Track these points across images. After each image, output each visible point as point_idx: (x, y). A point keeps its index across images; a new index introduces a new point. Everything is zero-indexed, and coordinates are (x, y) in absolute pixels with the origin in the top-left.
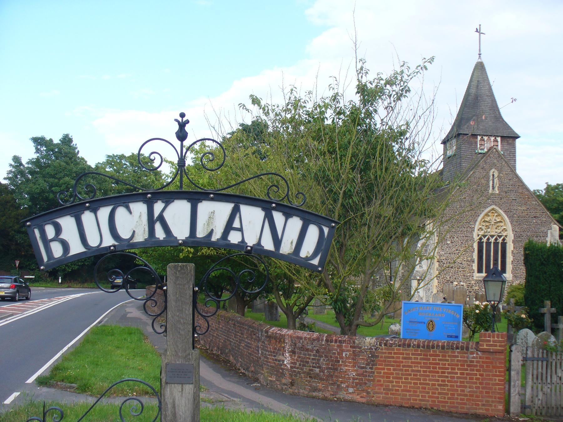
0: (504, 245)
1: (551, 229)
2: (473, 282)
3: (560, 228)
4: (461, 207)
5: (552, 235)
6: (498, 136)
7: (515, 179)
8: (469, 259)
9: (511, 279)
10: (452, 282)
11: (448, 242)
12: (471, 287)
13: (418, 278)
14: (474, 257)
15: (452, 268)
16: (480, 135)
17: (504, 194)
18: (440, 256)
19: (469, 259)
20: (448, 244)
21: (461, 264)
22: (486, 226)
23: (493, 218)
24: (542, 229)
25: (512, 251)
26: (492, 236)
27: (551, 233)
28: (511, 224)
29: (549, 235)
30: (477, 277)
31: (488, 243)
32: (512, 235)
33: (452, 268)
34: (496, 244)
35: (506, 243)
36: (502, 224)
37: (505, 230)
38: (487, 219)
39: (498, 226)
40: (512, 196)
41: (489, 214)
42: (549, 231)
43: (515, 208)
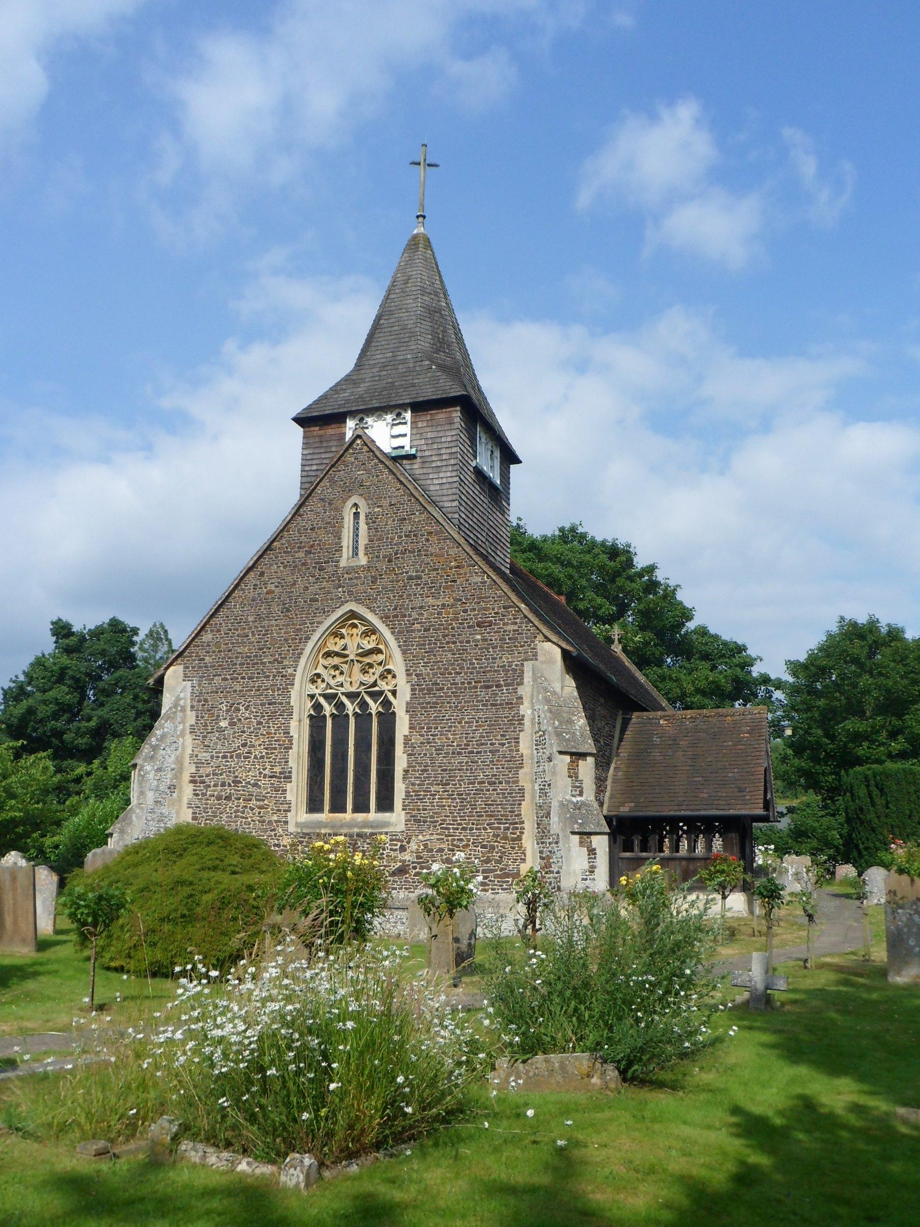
0: (388, 719)
1: (535, 657)
3: (564, 651)
4: (259, 618)
6: (404, 407)
8: (277, 769)
9: (401, 827)
11: (223, 724)
14: (292, 763)
15: (228, 798)
16: (352, 414)
18: (199, 764)
20: (221, 730)
22: (336, 667)
23: (354, 642)
25: (407, 739)
28: (404, 652)
31: (340, 719)
32: (408, 688)
33: (228, 798)
34: (363, 718)
35: (394, 714)
38: (335, 645)
39: (371, 666)
41: (343, 631)
42: (528, 666)
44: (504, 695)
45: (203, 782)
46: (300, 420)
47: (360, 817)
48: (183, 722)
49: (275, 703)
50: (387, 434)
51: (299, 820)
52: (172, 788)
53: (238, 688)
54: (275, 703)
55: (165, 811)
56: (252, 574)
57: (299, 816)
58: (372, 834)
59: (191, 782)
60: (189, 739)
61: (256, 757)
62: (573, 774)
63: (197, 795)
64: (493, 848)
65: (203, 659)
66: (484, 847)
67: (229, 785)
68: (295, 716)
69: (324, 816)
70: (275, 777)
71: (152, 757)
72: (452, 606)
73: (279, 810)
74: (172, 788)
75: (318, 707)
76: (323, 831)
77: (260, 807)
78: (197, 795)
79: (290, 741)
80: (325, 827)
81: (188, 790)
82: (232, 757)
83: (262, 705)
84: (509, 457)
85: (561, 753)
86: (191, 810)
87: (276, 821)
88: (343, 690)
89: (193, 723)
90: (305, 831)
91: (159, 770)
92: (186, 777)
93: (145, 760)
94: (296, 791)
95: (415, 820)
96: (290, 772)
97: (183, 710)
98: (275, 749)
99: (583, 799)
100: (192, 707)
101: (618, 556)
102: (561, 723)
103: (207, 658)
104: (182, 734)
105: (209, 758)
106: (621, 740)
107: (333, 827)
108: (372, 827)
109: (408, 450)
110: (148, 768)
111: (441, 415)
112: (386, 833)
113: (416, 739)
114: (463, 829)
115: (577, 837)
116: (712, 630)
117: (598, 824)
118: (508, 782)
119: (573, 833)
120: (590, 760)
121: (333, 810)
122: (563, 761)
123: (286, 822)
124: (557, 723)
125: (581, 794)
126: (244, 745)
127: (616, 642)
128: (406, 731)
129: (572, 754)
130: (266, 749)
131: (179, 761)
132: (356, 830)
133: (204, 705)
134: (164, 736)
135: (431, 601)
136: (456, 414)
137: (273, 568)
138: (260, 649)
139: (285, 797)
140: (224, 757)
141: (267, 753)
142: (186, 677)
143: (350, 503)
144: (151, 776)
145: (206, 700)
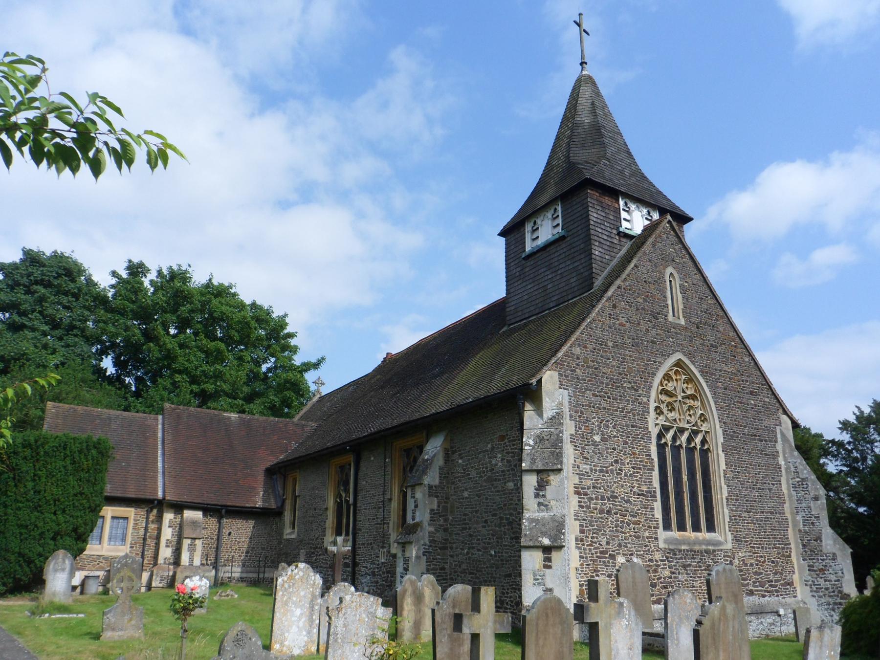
2: (658, 556)
7: (711, 301)
9: (729, 546)
10: (613, 557)
11: (597, 438)
12: (655, 571)
13: (546, 541)
17: (694, 329)
18: (581, 475)
19: (644, 488)
20: (595, 444)
21: (628, 501)
24: (766, 423)
26: (682, 430)
29: (779, 436)
30: (666, 541)
36: (697, 404)
37: (703, 418)
40: (710, 337)
43: (717, 366)
45: (586, 494)
47: (699, 534)
49: (636, 426)
53: (607, 406)
54: (636, 426)
58: (714, 551)
61: (626, 475)
63: (582, 507)
65: (575, 371)
67: (609, 499)
70: (643, 495)
73: (650, 527)
76: (683, 547)
77: (635, 523)
78: (582, 507)
79: (652, 463)
80: (684, 544)
81: (574, 500)
82: (607, 472)
83: (627, 426)
86: (578, 523)
87: (648, 538)
89: (573, 432)
90: (671, 547)
95: (737, 540)
96: (655, 492)
98: (640, 469)
100: (571, 416)
103: (578, 370)
105: (588, 470)
107: (689, 544)
108: (714, 545)
112: (722, 550)
114: (762, 548)
118: (780, 513)
121: (696, 528)
123: (657, 539)
126: (616, 462)
128: (723, 466)
130: (633, 468)
132: (704, 547)
133: (580, 416)
138: (621, 374)
139: (653, 515)
140: (601, 471)
141: (634, 472)
142: (561, 386)
145: (582, 412)
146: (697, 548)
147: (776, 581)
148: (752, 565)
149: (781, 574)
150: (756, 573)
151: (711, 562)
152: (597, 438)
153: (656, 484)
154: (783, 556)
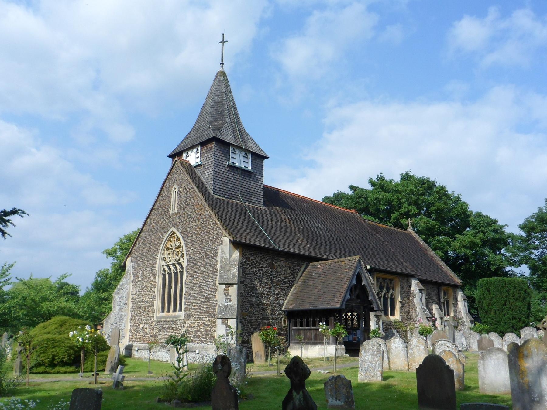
5: (223, 252)
6: (197, 145)
10: (139, 325)
18: (134, 295)
21: (147, 302)
27: (222, 249)
33: (140, 308)
44: (213, 261)
46: (168, 156)
48: (130, 279)
50: (193, 158)
51: (158, 315)
52: (125, 304)
55: (123, 313)
56: (148, 220)
57: (158, 314)
58: (176, 321)
59: (132, 302)
60: (131, 285)
62: (226, 293)
64: (208, 325)
66: (206, 325)
68: (157, 275)
69: (171, 313)
71: (118, 293)
72: (199, 225)
74: (125, 304)
75: (164, 270)
76: (163, 320)
81: (131, 304)
84: (259, 158)
85: (220, 284)
88: (171, 263)
91: (121, 298)
92: (130, 300)
93: (116, 294)
94: (157, 304)
95: (187, 314)
97: (130, 274)
99: (230, 303)
101: (427, 186)
102: (224, 271)
104: (129, 284)
106: (301, 275)
109: (200, 163)
110: (117, 297)
111: (209, 146)
113: (188, 281)
115: (220, 320)
116: (484, 213)
117: (232, 314)
119: (218, 318)
120: (235, 287)
122: (221, 288)
124: (222, 271)
125: (230, 301)
127: (410, 226)
129: (226, 284)
131: (128, 294)
132: (171, 319)
134: (122, 285)
135: (194, 224)
136: (213, 145)
137: (153, 217)
143: (173, 188)
144: (118, 300)
146: (168, 320)
147: (206, 335)
148: (194, 327)
149: (210, 331)
150: (196, 331)
151: (174, 326)
152: (140, 279)
153: (184, 289)
154: (212, 321)
